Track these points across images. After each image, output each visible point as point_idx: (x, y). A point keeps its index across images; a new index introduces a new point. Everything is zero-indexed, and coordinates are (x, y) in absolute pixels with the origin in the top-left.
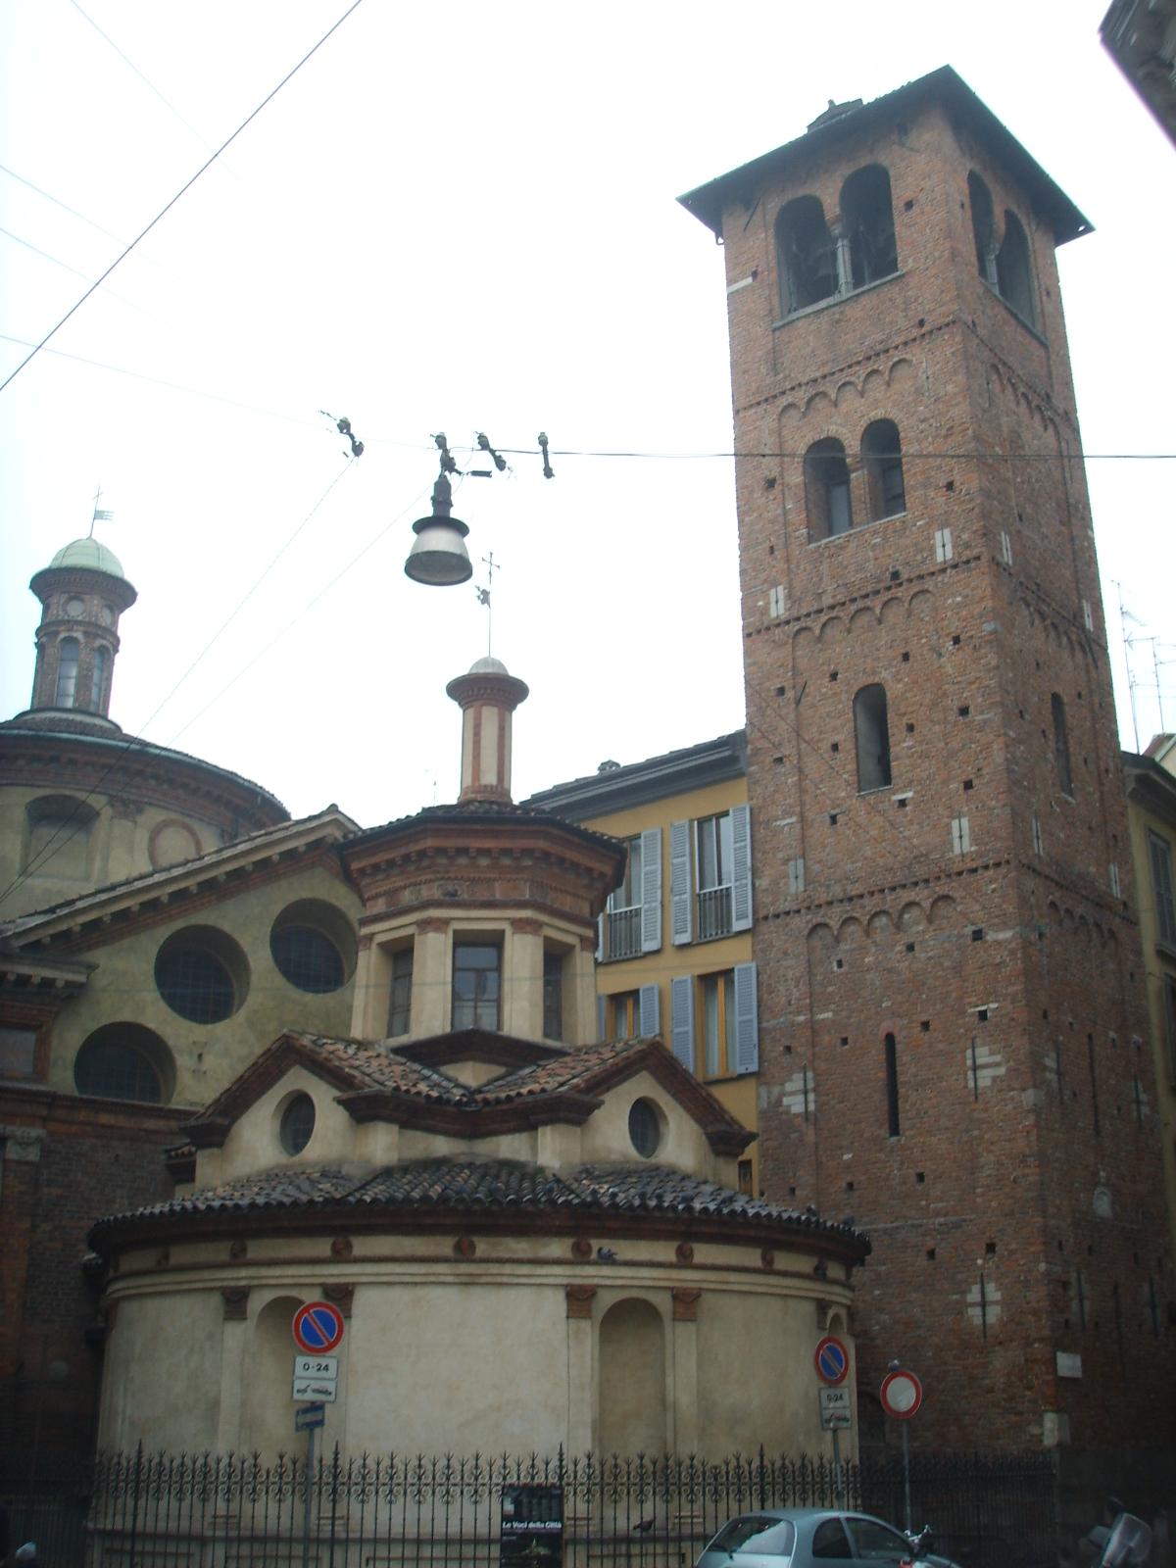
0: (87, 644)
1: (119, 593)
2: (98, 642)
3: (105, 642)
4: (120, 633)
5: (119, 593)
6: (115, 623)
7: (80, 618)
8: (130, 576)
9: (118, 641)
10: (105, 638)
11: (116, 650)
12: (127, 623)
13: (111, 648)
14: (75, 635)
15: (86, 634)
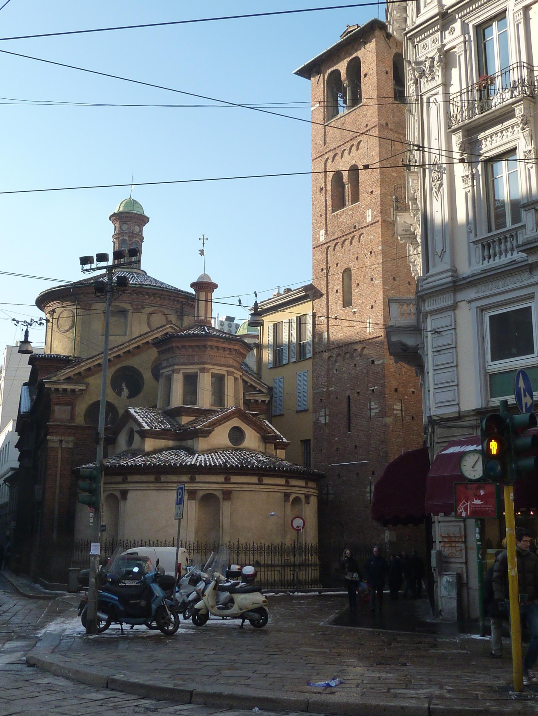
0: (130, 241)
1: (143, 220)
2: (134, 239)
3: (137, 239)
4: (143, 235)
5: (143, 220)
6: (141, 231)
7: (127, 231)
8: (146, 214)
9: (143, 238)
10: (136, 238)
11: (142, 241)
12: (146, 230)
13: (140, 241)
14: (125, 238)
15: (129, 237)
